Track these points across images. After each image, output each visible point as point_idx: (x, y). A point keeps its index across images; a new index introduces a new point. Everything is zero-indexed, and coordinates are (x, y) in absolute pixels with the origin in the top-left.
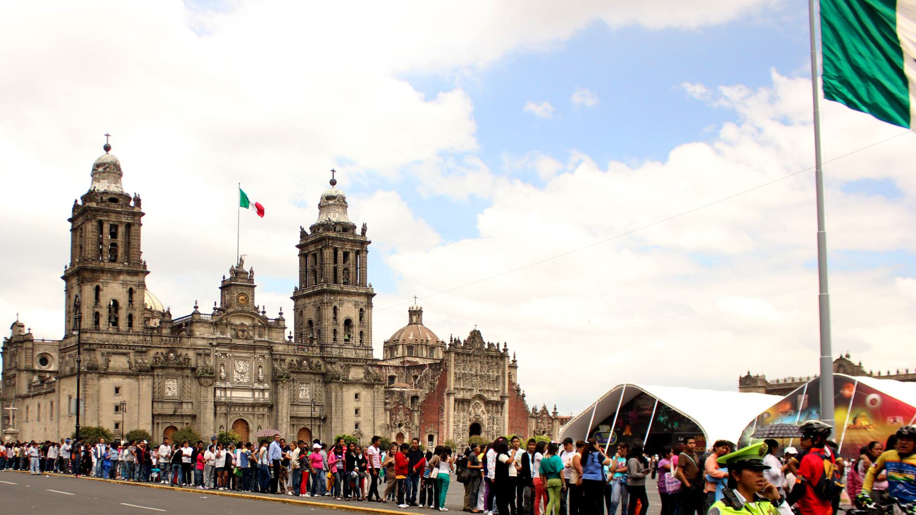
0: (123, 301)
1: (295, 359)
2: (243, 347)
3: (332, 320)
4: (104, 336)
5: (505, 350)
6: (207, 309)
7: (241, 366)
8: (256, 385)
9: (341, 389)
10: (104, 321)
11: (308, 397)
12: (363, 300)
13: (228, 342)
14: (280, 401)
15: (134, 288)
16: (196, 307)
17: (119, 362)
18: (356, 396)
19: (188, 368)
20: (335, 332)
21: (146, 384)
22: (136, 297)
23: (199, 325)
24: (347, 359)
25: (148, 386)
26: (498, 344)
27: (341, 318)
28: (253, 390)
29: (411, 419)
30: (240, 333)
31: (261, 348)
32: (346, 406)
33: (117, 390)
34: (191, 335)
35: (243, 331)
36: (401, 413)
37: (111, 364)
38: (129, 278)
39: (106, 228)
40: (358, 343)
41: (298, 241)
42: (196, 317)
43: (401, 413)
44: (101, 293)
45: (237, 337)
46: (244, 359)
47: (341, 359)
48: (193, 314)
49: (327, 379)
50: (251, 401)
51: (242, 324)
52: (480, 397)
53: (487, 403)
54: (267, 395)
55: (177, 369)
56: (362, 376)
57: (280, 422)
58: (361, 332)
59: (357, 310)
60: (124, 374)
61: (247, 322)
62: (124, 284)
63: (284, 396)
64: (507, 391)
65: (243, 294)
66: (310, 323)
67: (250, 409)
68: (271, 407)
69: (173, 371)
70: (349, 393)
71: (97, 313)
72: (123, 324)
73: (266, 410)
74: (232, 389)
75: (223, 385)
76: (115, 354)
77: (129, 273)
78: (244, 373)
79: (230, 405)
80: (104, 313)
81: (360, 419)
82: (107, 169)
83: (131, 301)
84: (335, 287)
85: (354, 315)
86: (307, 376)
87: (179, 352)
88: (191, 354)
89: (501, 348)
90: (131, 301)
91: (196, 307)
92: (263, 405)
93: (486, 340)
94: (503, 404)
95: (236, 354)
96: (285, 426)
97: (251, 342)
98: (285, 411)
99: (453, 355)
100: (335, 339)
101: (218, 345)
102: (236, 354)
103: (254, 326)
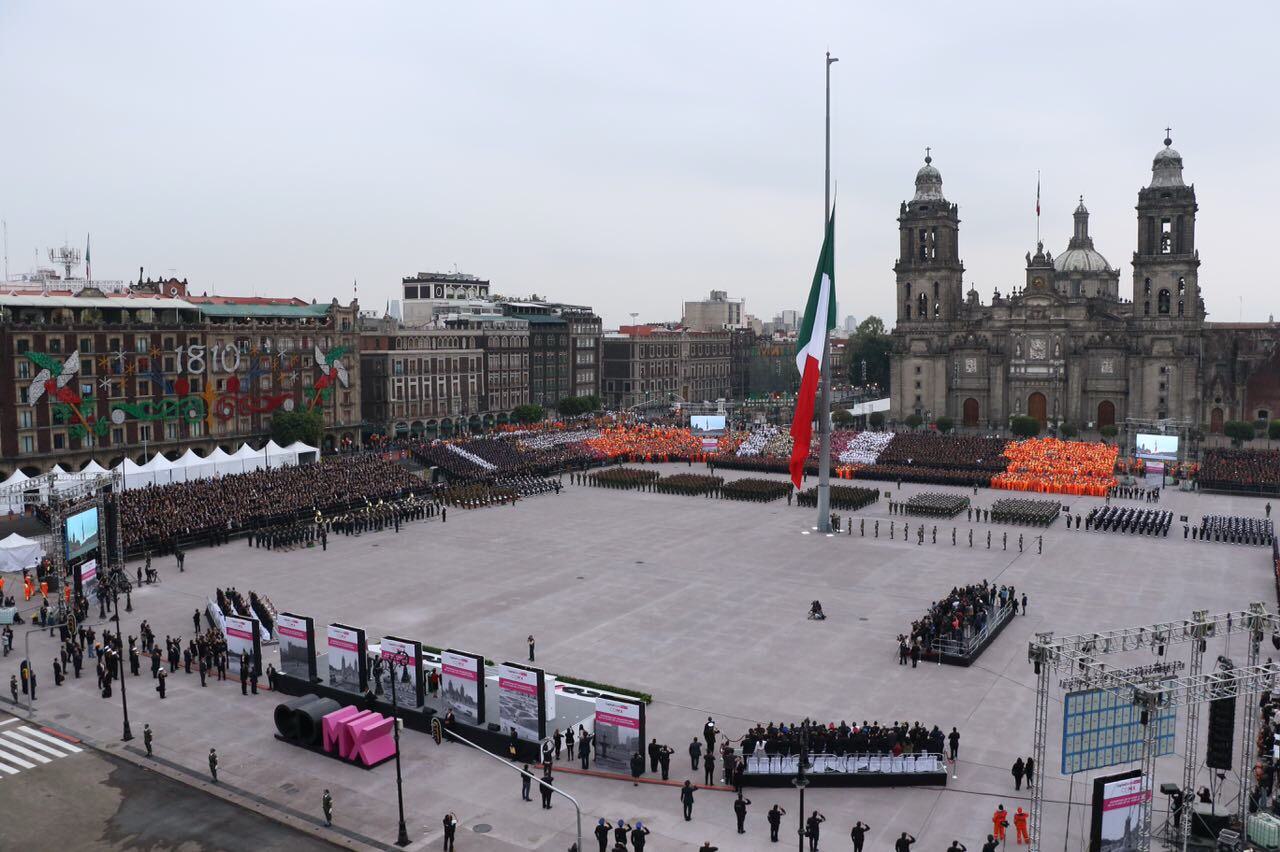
1: (1096, 335)
4: (913, 325)
7: (1038, 344)
8: (1052, 361)
9: (1143, 366)
11: (1111, 372)
12: (1182, 268)
18: (1163, 370)
21: (940, 365)
22: (942, 290)
24: (1158, 332)
28: (1048, 366)
29: (1233, 396)
30: (1036, 314)
31: (1055, 326)
32: (1147, 381)
33: (918, 370)
37: (912, 348)
38: (933, 274)
39: (916, 232)
46: (1040, 337)
47: (1152, 331)
49: (1129, 351)
50: (1045, 376)
54: (1062, 371)
57: (1070, 396)
60: (923, 356)
61: (1044, 303)
62: (931, 279)
63: (1076, 372)
65: (1038, 277)
67: (1046, 384)
68: (1065, 380)
71: (909, 306)
74: (1026, 366)
75: (1017, 362)
78: (1039, 350)
79: (1026, 380)
80: (914, 305)
82: (928, 180)
83: (936, 293)
88: (988, 335)
90: (936, 293)
95: (1032, 334)
96: (1075, 400)
97: (1046, 322)
98: (1075, 386)
100: (1147, 312)
102: (1032, 334)
103: (1050, 306)
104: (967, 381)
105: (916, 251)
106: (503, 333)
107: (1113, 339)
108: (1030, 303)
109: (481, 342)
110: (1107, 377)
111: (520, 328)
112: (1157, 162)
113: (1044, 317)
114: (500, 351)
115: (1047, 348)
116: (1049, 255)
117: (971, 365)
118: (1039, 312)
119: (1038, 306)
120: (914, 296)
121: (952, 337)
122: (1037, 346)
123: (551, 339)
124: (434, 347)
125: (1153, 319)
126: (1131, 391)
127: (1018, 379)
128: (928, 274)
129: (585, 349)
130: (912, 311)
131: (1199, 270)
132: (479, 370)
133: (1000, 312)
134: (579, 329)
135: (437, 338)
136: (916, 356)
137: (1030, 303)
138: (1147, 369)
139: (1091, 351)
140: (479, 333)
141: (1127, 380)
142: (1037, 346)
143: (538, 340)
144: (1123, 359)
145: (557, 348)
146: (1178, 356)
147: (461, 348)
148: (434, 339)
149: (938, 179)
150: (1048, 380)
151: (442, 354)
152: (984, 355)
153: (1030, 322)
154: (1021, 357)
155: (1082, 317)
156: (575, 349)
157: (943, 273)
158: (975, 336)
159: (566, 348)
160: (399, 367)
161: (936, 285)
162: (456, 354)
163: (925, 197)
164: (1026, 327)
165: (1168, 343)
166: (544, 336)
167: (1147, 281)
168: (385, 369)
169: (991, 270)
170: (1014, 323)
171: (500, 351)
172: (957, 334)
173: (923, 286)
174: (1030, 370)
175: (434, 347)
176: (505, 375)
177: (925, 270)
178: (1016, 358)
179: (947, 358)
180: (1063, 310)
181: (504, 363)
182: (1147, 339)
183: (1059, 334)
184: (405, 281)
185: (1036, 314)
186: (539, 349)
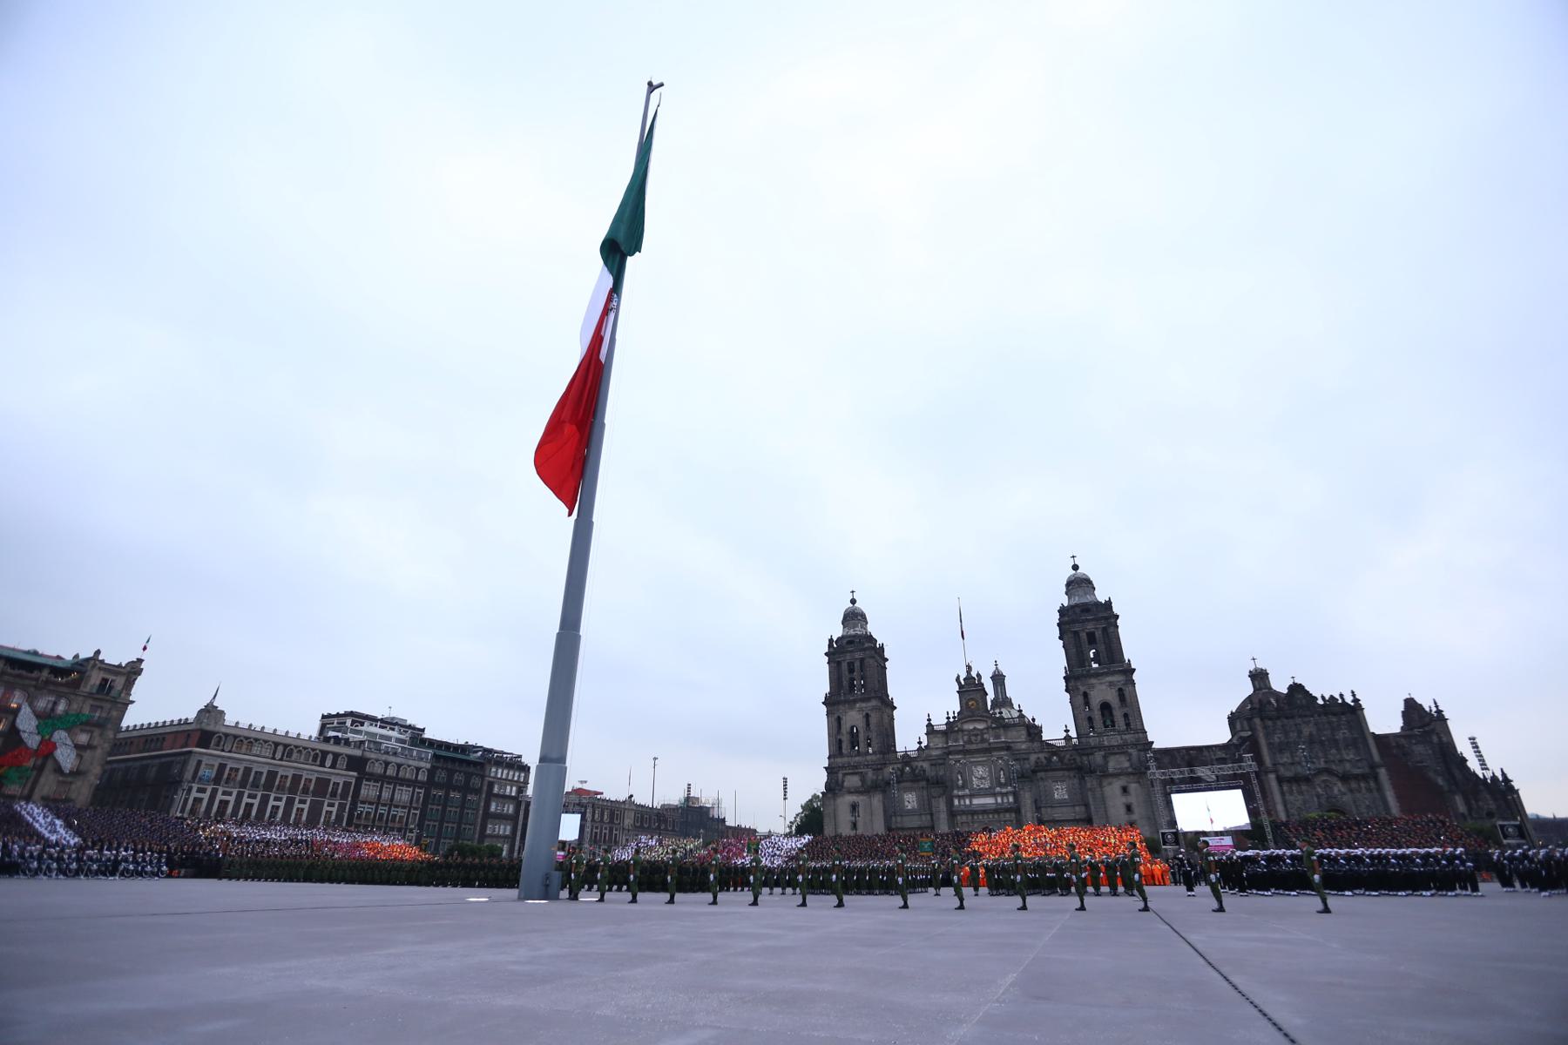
1: (1042, 756)
2: (978, 751)
4: (845, 760)
5: (1356, 700)
7: (980, 771)
9: (1101, 786)
17: (853, 781)
18: (1125, 790)
20: (1090, 719)
21: (877, 800)
22: (873, 720)
28: (994, 795)
39: (844, 666)
45: (970, 742)
47: (1100, 748)
52: (1328, 771)
53: (1345, 778)
56: (1127, 764)
58: (1126, 716)
60: (857, 792)
61: (980, 726)
62: (861, 710)
64: (1377, 758)
70: (1113, 789)
74: (971, 796)
77: (863, 700)
79: (973, 812)
80: (845, 738)
81: (1134, 817)
82: (854, 617)
85: (1111, 697)
92: (1007, 810)
94: (1376, 778)
97: (985, 745)
99: (1257, 721)
101: (950, 753)
104: (905, 819)
105: (845, 683)
106: (384, 757)
107: (1061, 760)
108: (966, 727)
109: (357, 764)
110: (1062, 803)
111: (422, 761)
112: (1069, 584)
114: (382, 779)
116: (979, 675)
117: (910, 800)
120: (845, 728)
122: (980, 774)
123: (459, 778)
124: (278, 755)
125: (1100, 735)
126: (1094, 818)
127: (963, 813)
129: (504, 797)
130: (844, 746)
131: (1135, 677)
132: (344, 796)
134: (501, 773)
135: (286, 746)
136: (850, 792)
137: (966, 727)
138: (1108, 790)
139: (1040, 775)
140: (358, 753)
141: (1087, 805)
142: (980, 774)
143: (441, 776)
144: (1076, 781)
145: (466, 789)
147: (322, 764)
148: (280, 748)
149: (863, 616)
150: (997, 811)
151: (286, 769)
153: (968, 747)
154: (963, 787)
155: (1023, 738)
156: (490, 795)
157: (874, 703)
159: (478, 791)
160: (207, 772)
161: (867, 716)
162: (311, 772)
163: (852, 632)
164: (965, 752)
165: (1123, 758)
166: (451, 773)
167: (1085, 695)
168: (181, 773)
169: (920, 705)
171: (382, 779)
173: (853, 718)
174: (975, 801)
175: (278, 755)
176: (382, 810)
177: (855, 701)
178: (959, 788)
179: (884, 792)
180: (1002, 731)
181: (386, 795)
182: (1098, 757)
184: (324, 717)
186: (439, 786)
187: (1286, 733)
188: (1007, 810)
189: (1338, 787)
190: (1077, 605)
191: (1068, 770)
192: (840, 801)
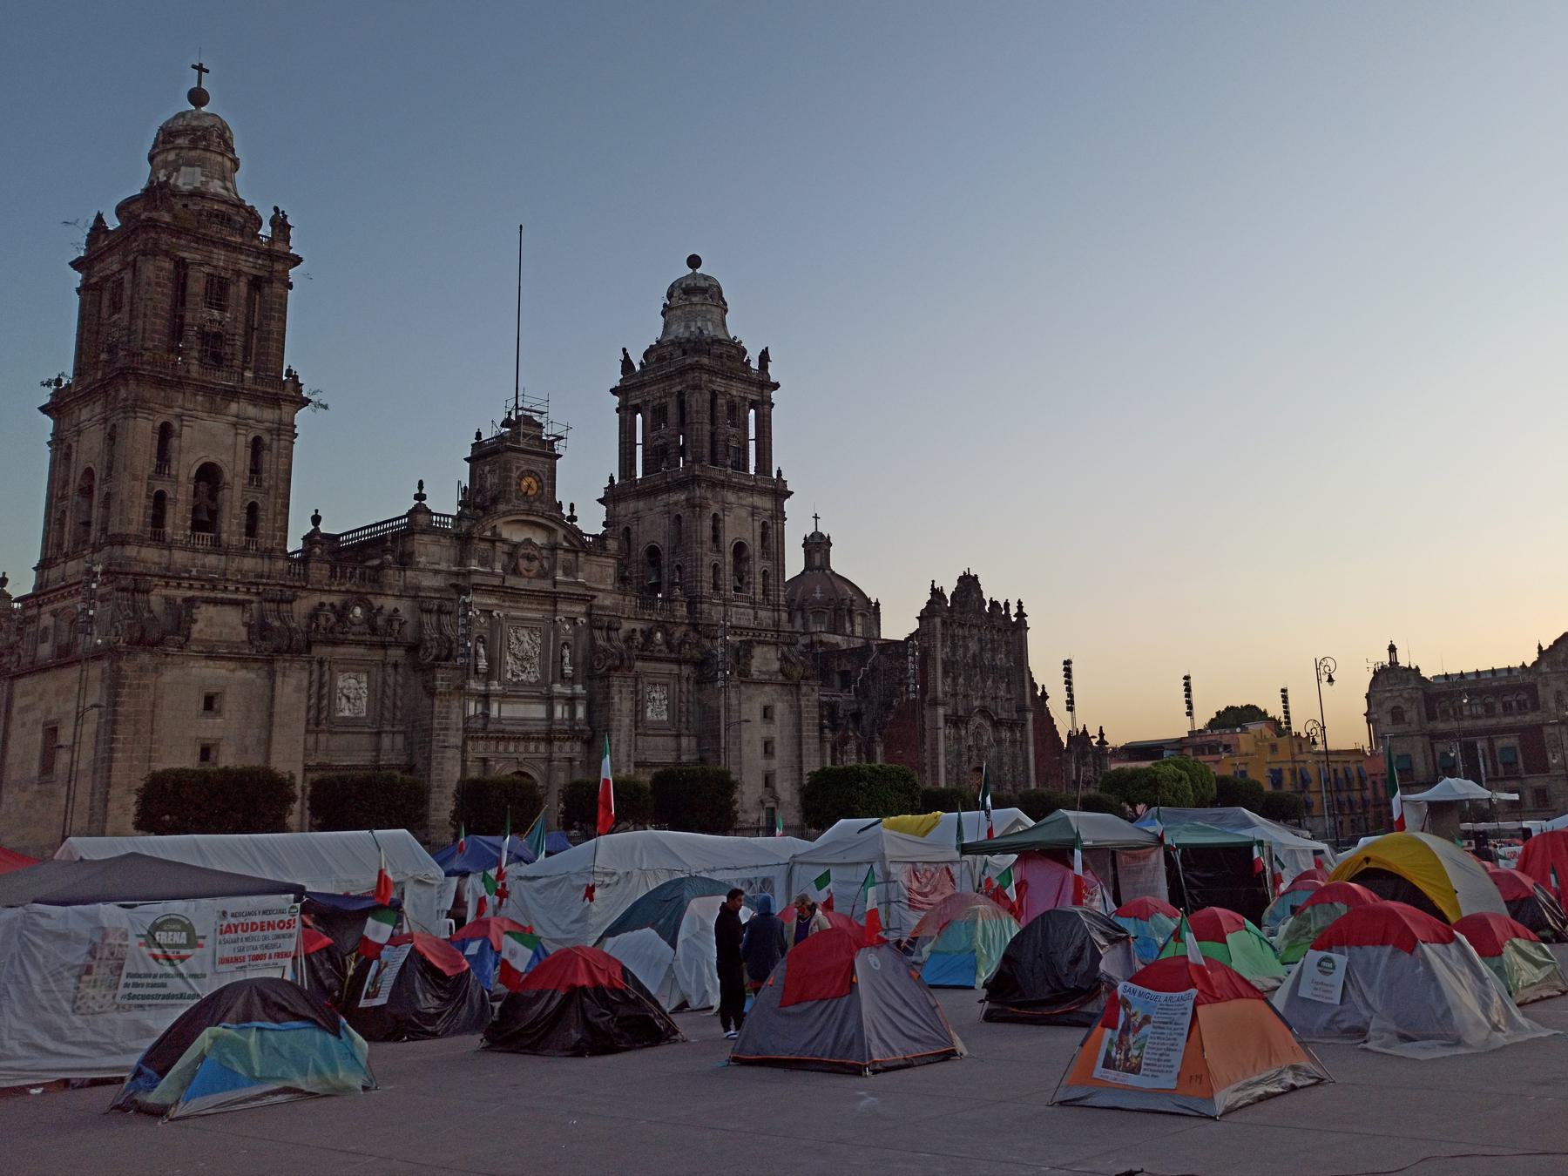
0: (235, 466)
1: (638, 626)
2: (531, 595)
3: (709, 544)
5: (1021, 615)
6: (445, 503)
8: (558, 688)
10: (177, 519)
12: (765, 503)
13: (497, 582)
14: (615, 724)
15: (266, 438)
16: (420, 497)
18: (767, 713)
19: (398, 645)
21: (292, 686)
23: (426, 538)
25: (297, 689)
26: (1007, 604)
27: (729, 538)
28: (549, 700)
30: (523, 563)
33: (210, 703)
34: (405, 561)
35: (530, 559)
36: (852, 746)
38: (251, 411)
40: (759, 597)
41: (616, 378)
42: (422, 519)
43: (852, 746)
44: (174, 442)
45: (516, 572)
48: (411, 513)
51: (528, 542)
53: (997, 724)
54: (580, 712)
55: (371, 646)
59: (757, 525)
61: (539, 538)
63: (622, 704)
65: (530, 473)
66: (653, 552)
69: (361, 650)
72: (231, 527)
73: (578, 747)
74: (504, 697)
76: (208, 601)
78: (528, 659)
81: (775, 764)
84: (716, 473)
86: (665, 667)
87: (377, 602)
88: (404, 607)
89: (1013, 610)
90: (255, 469)
91: (420, 497)
93: (986, 597)
95: (514, 613)
97: (546, 585)
100: (716, 587)
101: (476, 588)
103: (553, 548)
107: (668, 643)
110: (657, 729)
113: (543, 575)
115: (543, 655)
118: (530, 559)
119: (528, 542)
120: (186, 464)
121: (304, 605)
128: (234, 407)
133: (434, 549)
136: (211, 655)
142: (523, 650)
146: (789, 682)
152: (395, 666)
153: (511, 581)
154: (489, 676)
158: (368, 608)
170: (476, 579)
172: (316, 599)
177: (232, 394)
183: (573, 621)
185: (523, 563)
187: (954, 648)
188: (573, 735)
189: (988, 734)
190: (677, 343)
191: (679, 662)
192: (169, 676)
